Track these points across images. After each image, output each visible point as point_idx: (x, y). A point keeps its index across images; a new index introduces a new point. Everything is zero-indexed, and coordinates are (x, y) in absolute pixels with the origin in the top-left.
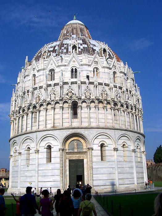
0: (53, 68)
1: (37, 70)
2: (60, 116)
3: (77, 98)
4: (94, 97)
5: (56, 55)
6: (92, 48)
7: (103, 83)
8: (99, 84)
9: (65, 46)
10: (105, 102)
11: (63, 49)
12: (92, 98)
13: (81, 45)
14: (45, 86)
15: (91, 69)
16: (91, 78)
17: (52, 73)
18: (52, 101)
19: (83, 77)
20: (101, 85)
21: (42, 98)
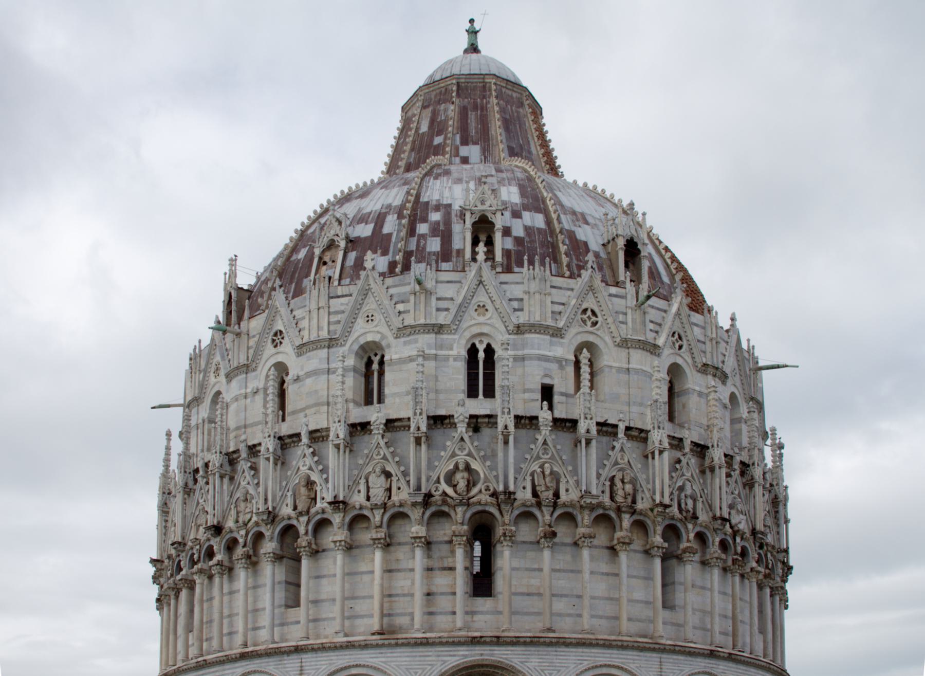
0: (377, 338)
1: (298, 342)
2: (413, 584)
3: (493, 500)
4: (574, 495)
5: (392, 265)
6: (571, 235)
7: (622, 427)
8: (599, 432)
9: (435, 217)
10: (627, 520)
11: (423, 236)
12: (564, 497)
13: (516, 215)
14: (339, 431)
15: (564, 350)
16: (563, 399)
17: (369, 363)
18: (374, 507)
19: (525, 391)
20: (607, 434)
21: (326, 494)
